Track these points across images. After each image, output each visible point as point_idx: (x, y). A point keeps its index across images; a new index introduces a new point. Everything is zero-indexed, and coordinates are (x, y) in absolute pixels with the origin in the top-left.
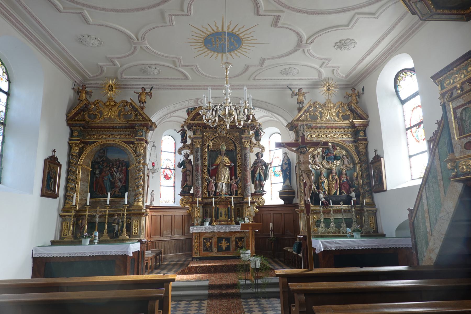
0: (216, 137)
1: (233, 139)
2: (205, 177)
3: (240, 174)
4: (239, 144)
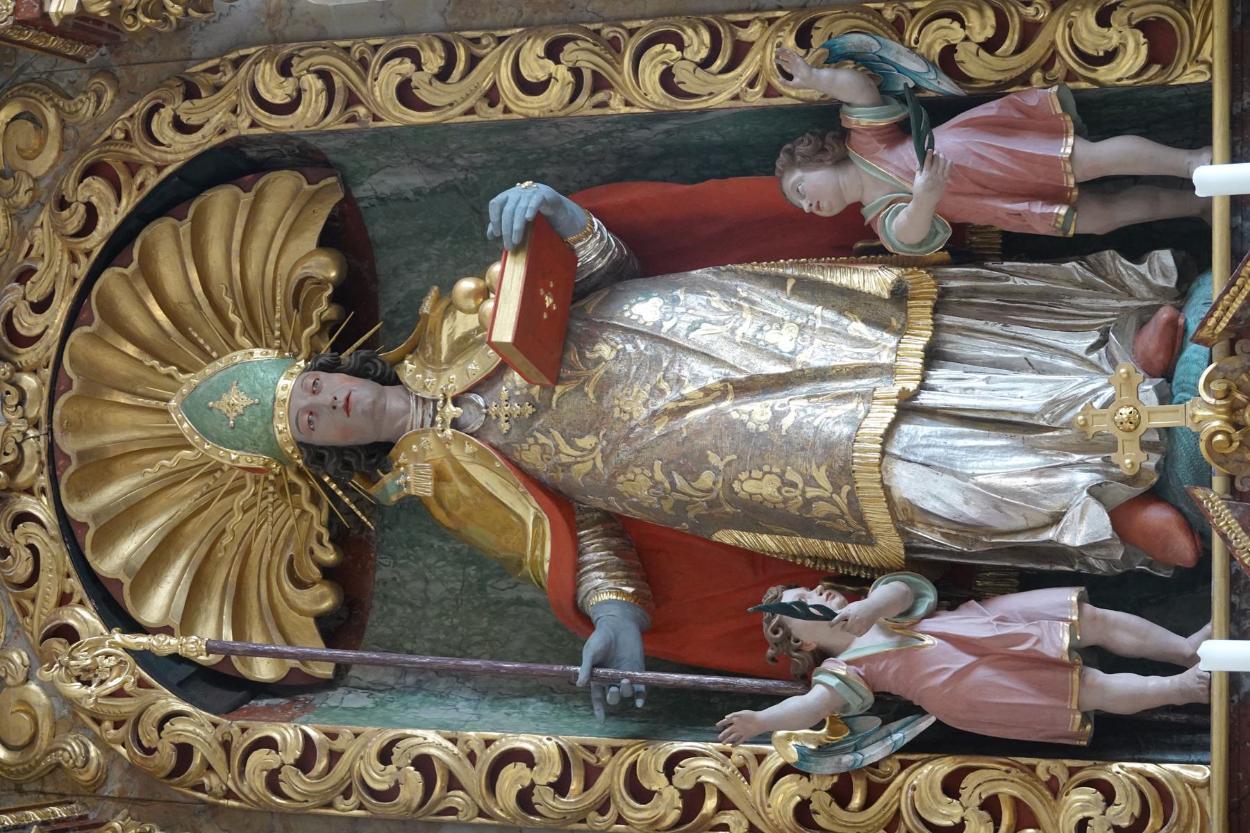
0: (69, 530)
1: (92, 215)
2: (789, 791)
3: (741, 51)
4: (191, 92)
